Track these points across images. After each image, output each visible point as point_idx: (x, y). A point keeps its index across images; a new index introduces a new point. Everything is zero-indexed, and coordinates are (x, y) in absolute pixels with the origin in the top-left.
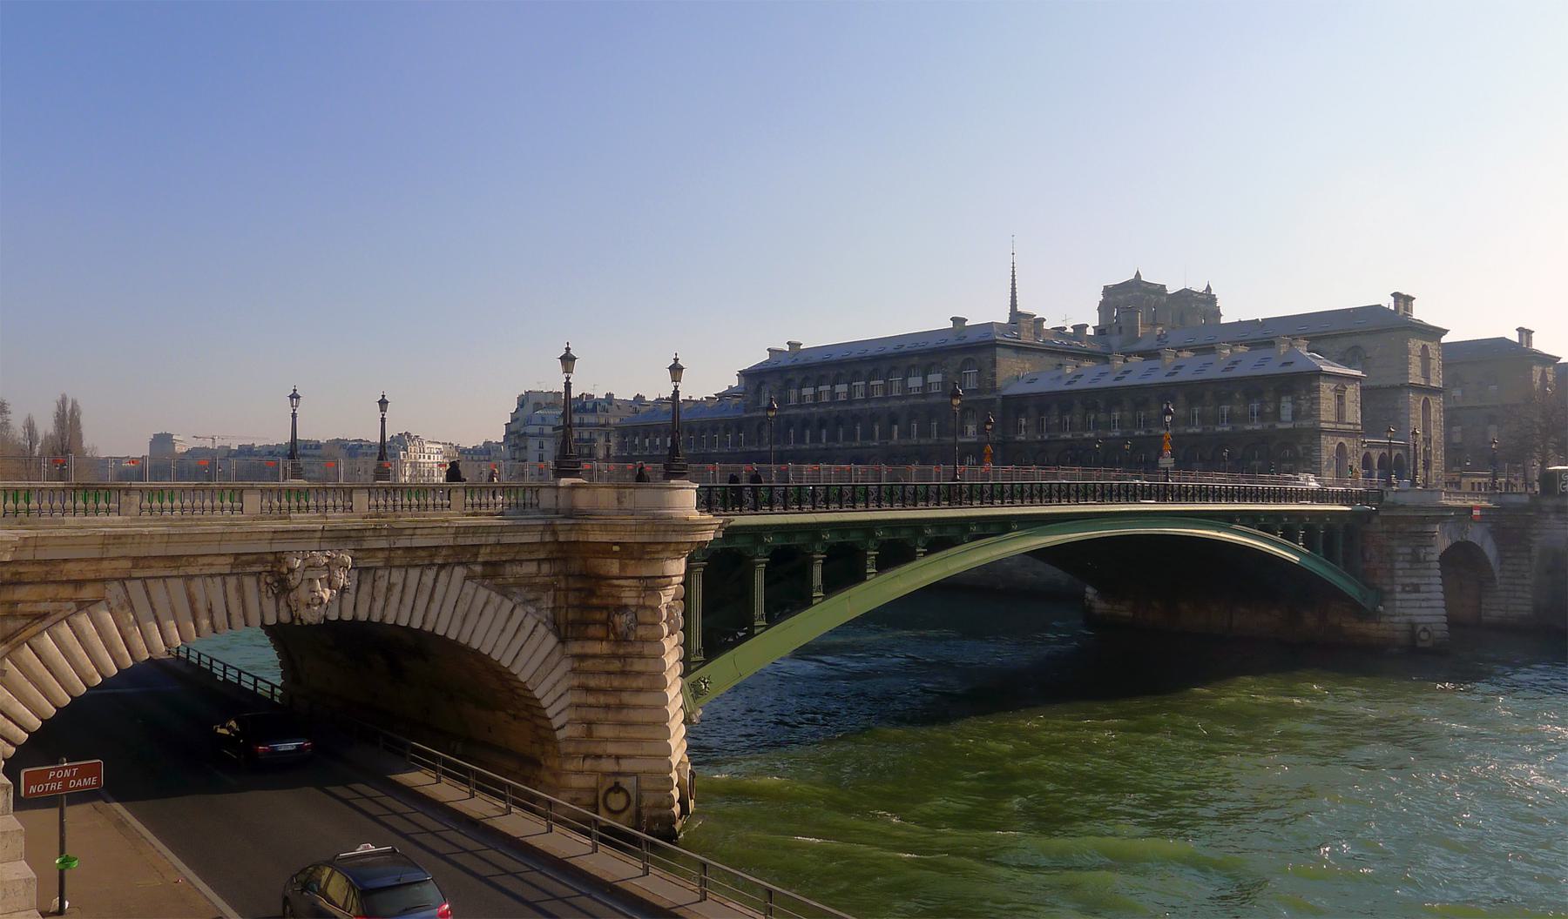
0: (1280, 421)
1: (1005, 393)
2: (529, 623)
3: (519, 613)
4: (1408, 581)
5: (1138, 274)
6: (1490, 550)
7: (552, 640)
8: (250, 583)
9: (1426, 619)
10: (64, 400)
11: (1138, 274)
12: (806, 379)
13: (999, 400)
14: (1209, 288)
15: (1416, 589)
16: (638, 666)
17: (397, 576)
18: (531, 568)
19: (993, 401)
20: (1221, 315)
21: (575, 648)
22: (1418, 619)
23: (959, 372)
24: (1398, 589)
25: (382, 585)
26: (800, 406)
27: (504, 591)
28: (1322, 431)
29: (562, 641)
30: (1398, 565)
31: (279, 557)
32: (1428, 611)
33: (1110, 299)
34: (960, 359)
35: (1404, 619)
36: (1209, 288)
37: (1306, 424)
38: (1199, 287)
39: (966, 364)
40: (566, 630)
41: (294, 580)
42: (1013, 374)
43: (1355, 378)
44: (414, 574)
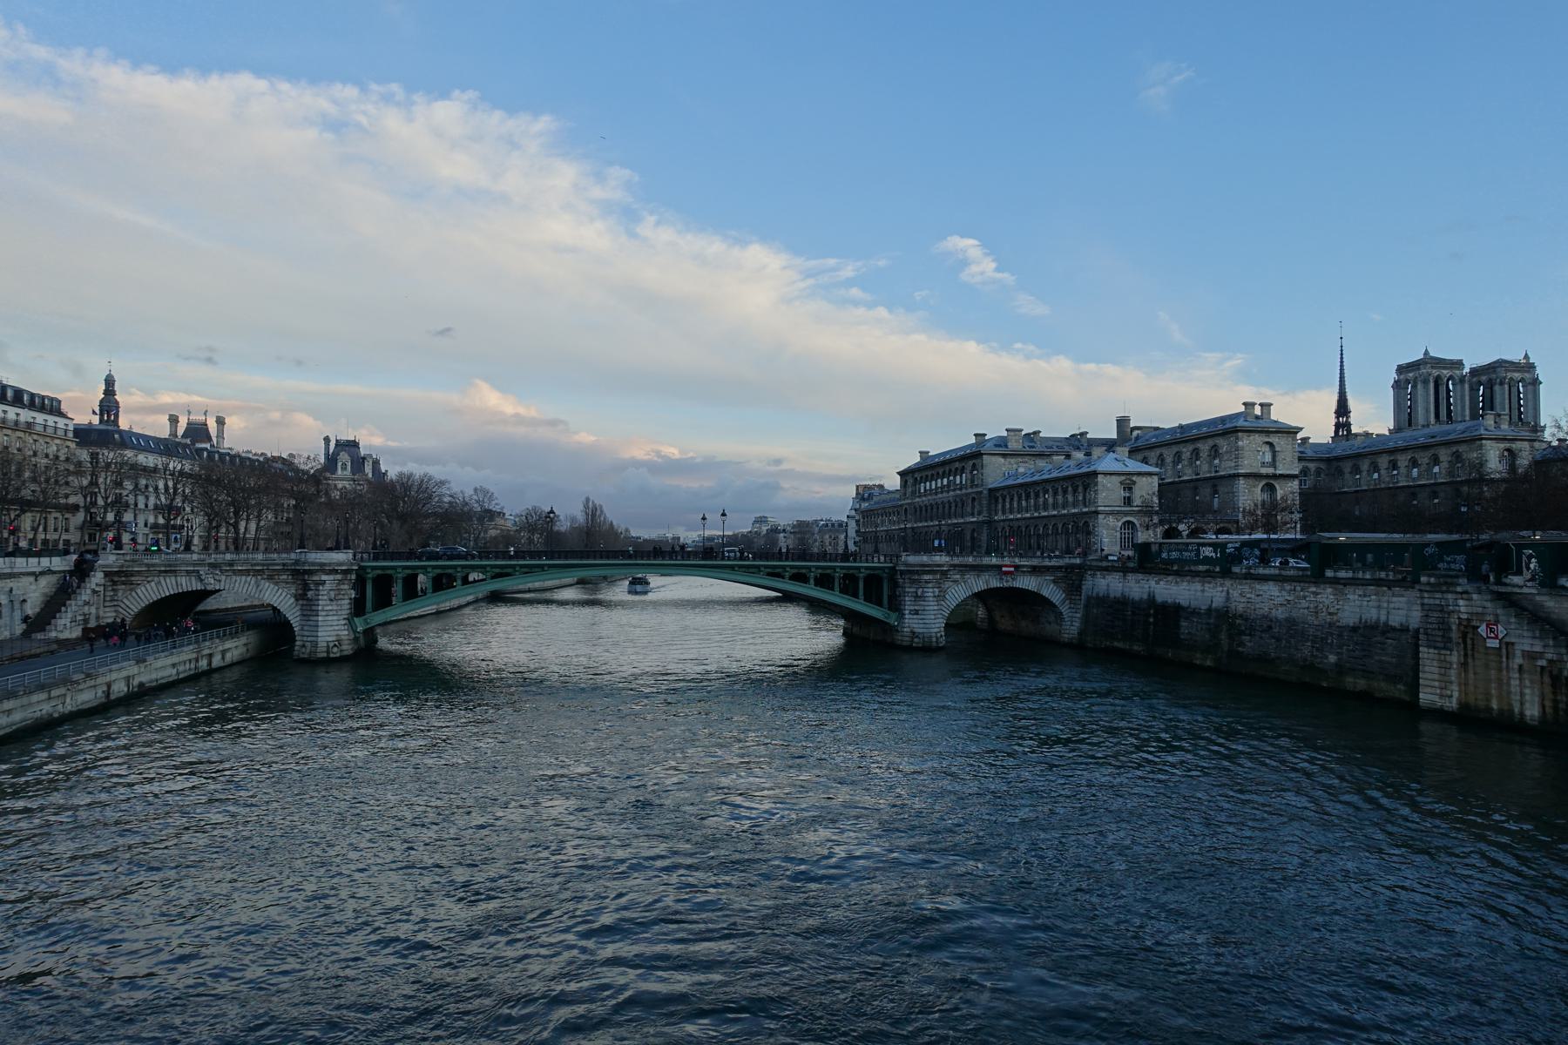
0: (1086, 506)
1: (990, 486)
2: (284, 594)
3: (280, 591)
4: (912, 608)
5: (1426, 353)
6: (1052, 592)
7: (293, 600)
8: (193, 578)
9: (921, 631)
10: (588, 500)
11: (1426, 353)
12: (921, 478)
13: (985, 492)
14: (1526, 357)
15: (917, 612)
16: (314, 608)
17: (238, 578)
18: (285, 577)
19: (981, 492)
20: (1541, 383)
21: (301, 602)
22: (916, 630)
23: (971, 472)
24: (907, 612)
25: (233, 580)
26: (919, 497)
27: (276, 584)
28: (1097, 513)
29: (297, 600)
30: (907, 598)
31: (198, 571)
32: (921, 626)
33: (1402, 377)
34: (971, 463)
35: (908, 630)
36: (1526, 357)
37: (1093, 509)
38: (1516, 356)
39: (974, 467)
40: (298, 598)
41: (203, 577)
42: (996, 472)
43: (1150, 474)
44: (244, 578)
